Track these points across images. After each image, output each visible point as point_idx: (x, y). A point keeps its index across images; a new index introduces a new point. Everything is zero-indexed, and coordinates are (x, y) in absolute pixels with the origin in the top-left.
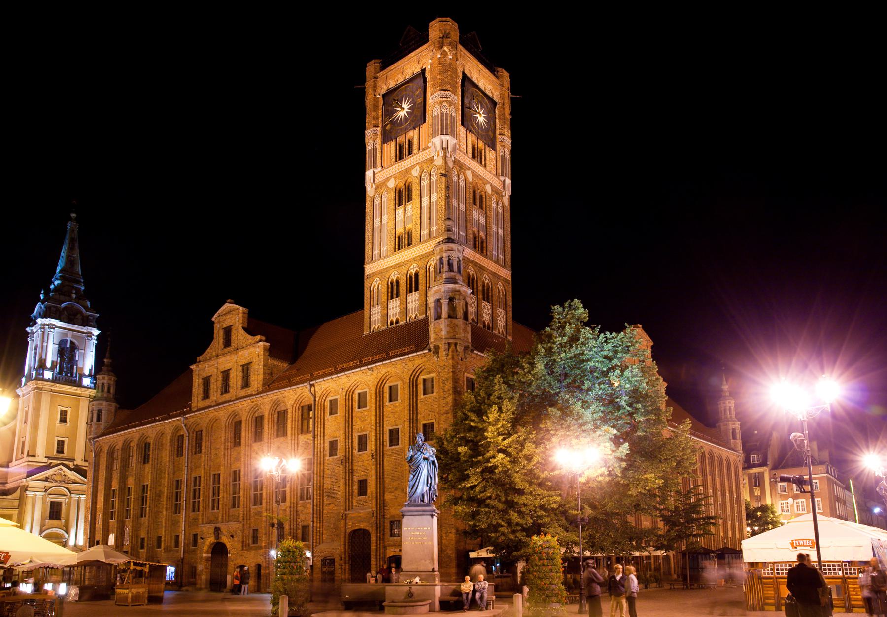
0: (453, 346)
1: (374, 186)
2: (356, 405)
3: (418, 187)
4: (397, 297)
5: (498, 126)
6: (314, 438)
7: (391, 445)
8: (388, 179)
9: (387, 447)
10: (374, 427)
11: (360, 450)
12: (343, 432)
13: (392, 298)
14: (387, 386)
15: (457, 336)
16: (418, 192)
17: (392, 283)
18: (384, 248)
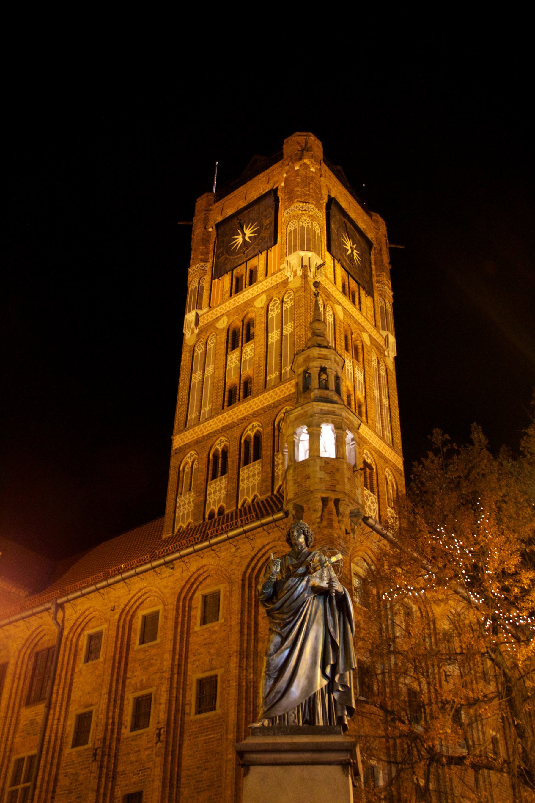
0: (331, 505)
1: (196, 331)
2: (136, 638)
3: (264, 320)
4: (224, 472)
5: (374, 273)
6: (49, 707)
7: (199, 711)
8: (217, 319)
9: (192, 715)
10: (167, 675)
11: (135, 726)
12: (105, 690)
13: (214, 477)
14: (198, 596)
15: (338, 487)
16: (263, 326)
17: (215, 456)
18: (206, 409)
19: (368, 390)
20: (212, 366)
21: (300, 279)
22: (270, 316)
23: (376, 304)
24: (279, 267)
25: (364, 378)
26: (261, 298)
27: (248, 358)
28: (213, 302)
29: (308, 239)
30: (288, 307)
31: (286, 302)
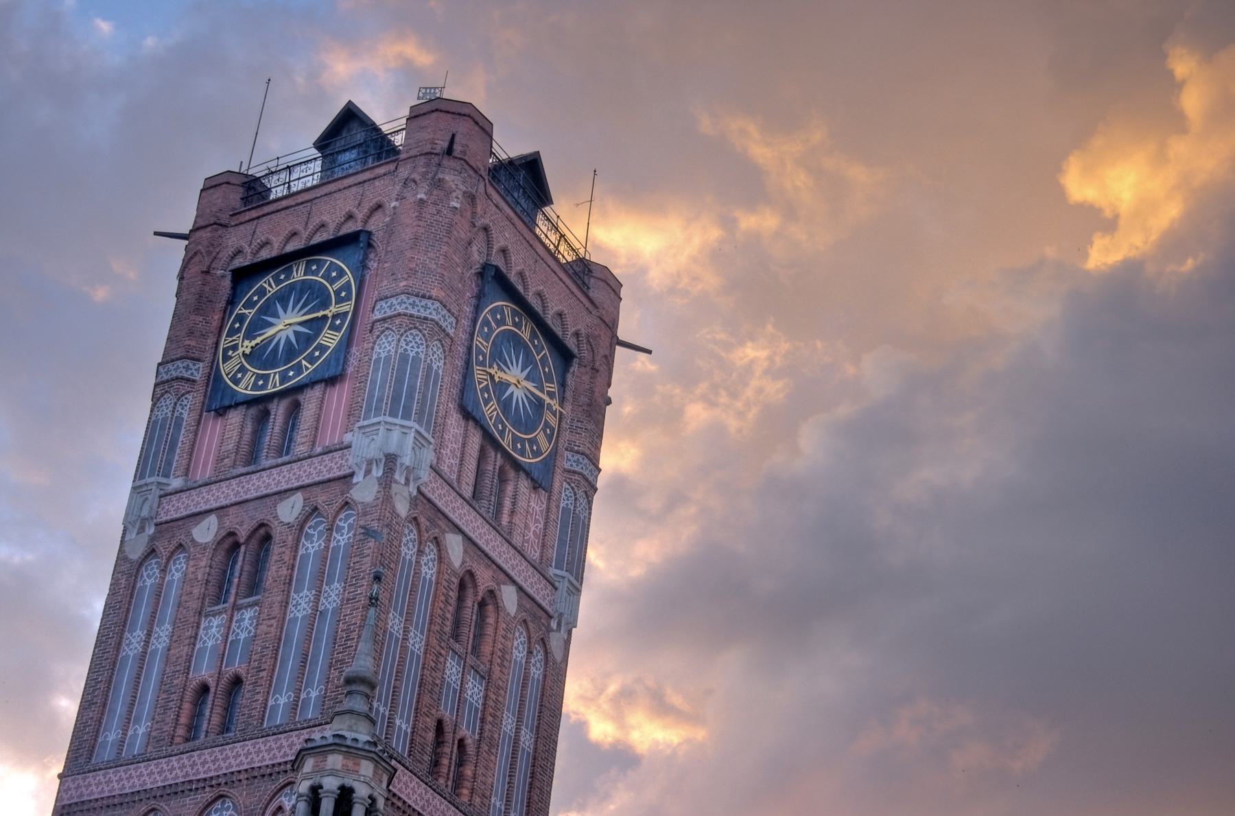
19: (487, 727)
20: (168, 626)
21: (376, 488)
22: (301, 552)
23: (553, 505)
24: (341, 436)
25: (486, 697)
26: (293, 498)
27: (242, 636)
28: (196, 467)
29: (412, 389)
30: (342, 543)
31: (339, 529)
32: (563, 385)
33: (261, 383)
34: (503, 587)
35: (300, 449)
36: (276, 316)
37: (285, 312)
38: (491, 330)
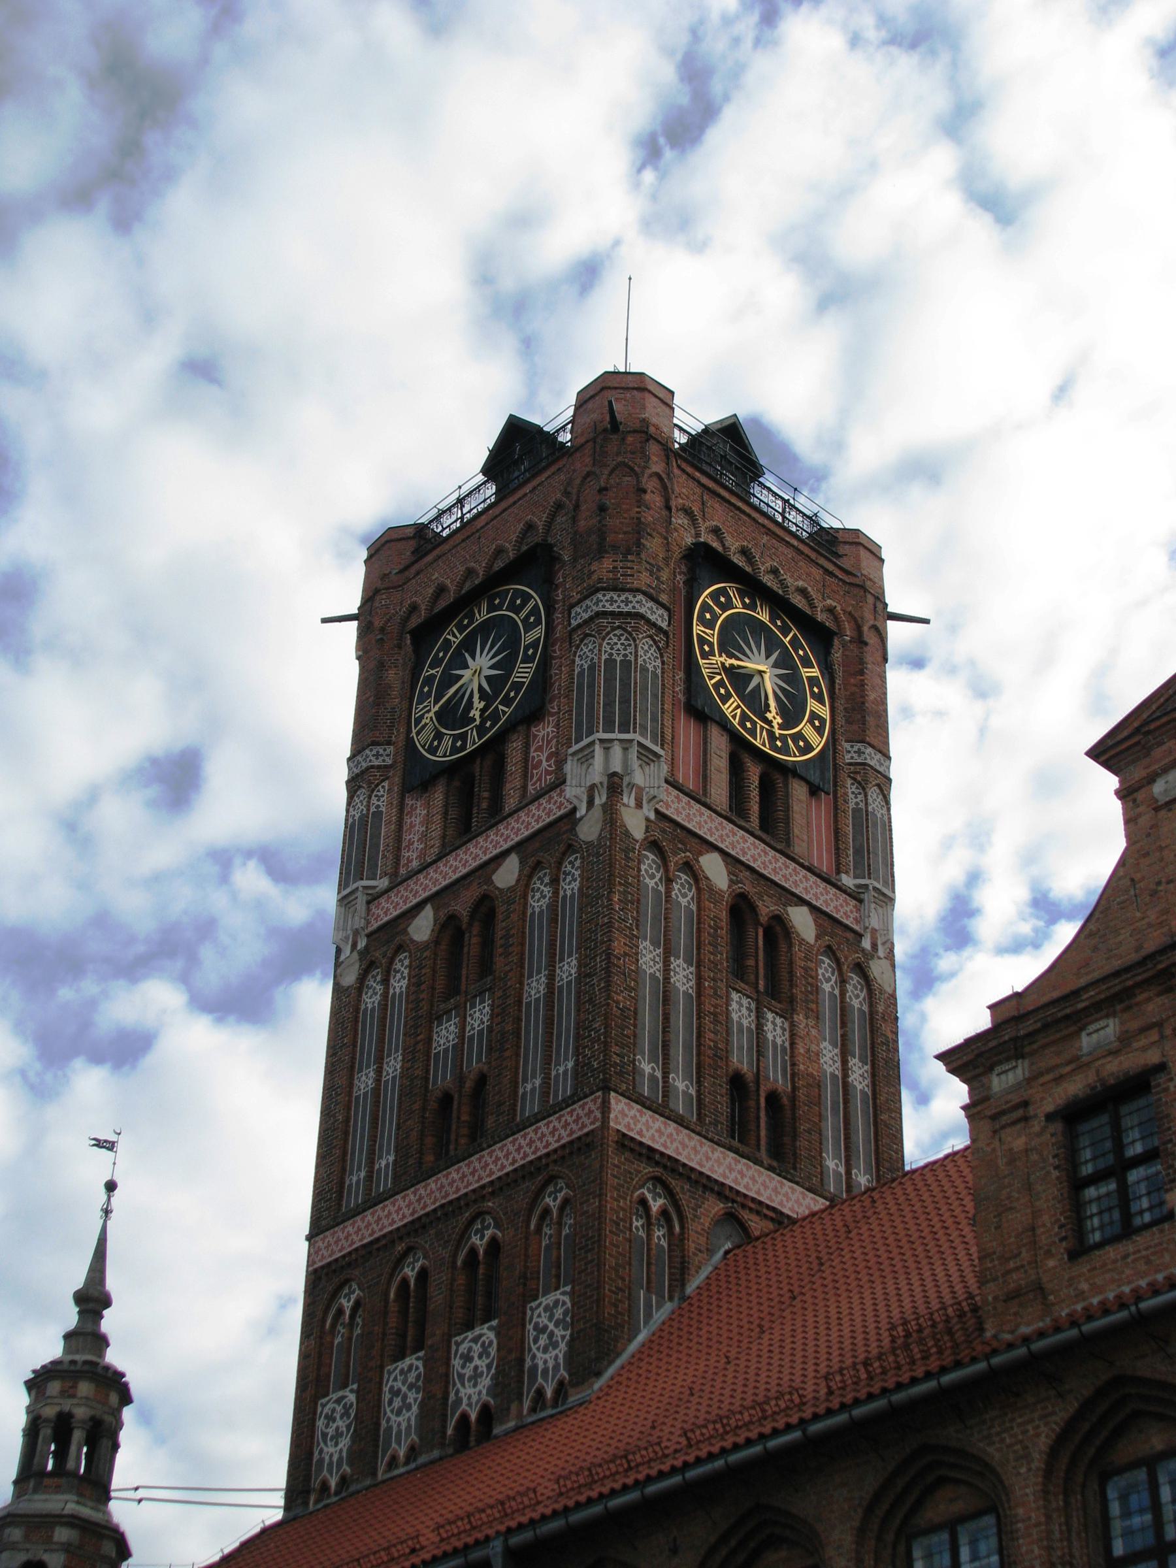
32: (827, 668)
33: (459, 744)
34: (790, 909)
35: (511, 802)
36: (466, 667)
37: (474, 658)
38: (715, 617)
